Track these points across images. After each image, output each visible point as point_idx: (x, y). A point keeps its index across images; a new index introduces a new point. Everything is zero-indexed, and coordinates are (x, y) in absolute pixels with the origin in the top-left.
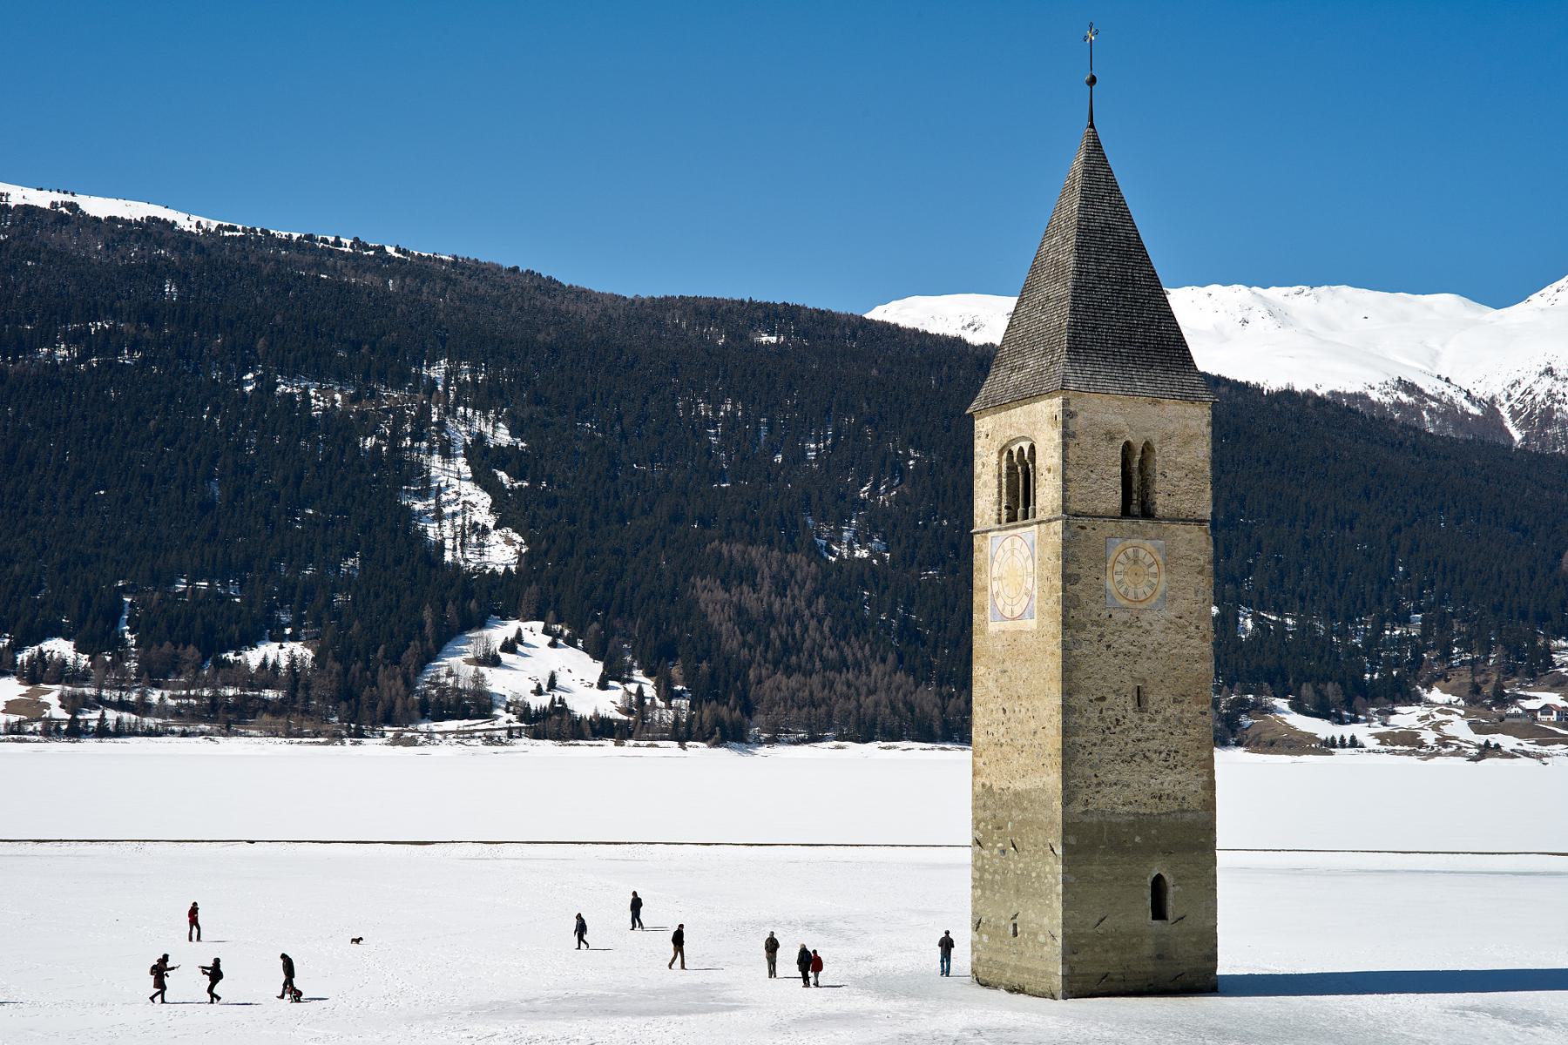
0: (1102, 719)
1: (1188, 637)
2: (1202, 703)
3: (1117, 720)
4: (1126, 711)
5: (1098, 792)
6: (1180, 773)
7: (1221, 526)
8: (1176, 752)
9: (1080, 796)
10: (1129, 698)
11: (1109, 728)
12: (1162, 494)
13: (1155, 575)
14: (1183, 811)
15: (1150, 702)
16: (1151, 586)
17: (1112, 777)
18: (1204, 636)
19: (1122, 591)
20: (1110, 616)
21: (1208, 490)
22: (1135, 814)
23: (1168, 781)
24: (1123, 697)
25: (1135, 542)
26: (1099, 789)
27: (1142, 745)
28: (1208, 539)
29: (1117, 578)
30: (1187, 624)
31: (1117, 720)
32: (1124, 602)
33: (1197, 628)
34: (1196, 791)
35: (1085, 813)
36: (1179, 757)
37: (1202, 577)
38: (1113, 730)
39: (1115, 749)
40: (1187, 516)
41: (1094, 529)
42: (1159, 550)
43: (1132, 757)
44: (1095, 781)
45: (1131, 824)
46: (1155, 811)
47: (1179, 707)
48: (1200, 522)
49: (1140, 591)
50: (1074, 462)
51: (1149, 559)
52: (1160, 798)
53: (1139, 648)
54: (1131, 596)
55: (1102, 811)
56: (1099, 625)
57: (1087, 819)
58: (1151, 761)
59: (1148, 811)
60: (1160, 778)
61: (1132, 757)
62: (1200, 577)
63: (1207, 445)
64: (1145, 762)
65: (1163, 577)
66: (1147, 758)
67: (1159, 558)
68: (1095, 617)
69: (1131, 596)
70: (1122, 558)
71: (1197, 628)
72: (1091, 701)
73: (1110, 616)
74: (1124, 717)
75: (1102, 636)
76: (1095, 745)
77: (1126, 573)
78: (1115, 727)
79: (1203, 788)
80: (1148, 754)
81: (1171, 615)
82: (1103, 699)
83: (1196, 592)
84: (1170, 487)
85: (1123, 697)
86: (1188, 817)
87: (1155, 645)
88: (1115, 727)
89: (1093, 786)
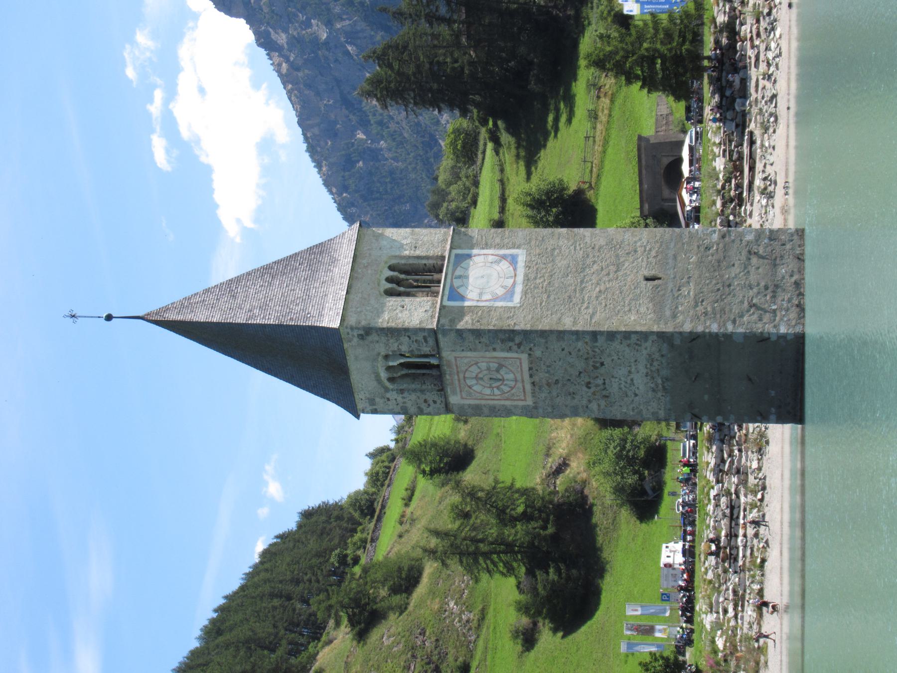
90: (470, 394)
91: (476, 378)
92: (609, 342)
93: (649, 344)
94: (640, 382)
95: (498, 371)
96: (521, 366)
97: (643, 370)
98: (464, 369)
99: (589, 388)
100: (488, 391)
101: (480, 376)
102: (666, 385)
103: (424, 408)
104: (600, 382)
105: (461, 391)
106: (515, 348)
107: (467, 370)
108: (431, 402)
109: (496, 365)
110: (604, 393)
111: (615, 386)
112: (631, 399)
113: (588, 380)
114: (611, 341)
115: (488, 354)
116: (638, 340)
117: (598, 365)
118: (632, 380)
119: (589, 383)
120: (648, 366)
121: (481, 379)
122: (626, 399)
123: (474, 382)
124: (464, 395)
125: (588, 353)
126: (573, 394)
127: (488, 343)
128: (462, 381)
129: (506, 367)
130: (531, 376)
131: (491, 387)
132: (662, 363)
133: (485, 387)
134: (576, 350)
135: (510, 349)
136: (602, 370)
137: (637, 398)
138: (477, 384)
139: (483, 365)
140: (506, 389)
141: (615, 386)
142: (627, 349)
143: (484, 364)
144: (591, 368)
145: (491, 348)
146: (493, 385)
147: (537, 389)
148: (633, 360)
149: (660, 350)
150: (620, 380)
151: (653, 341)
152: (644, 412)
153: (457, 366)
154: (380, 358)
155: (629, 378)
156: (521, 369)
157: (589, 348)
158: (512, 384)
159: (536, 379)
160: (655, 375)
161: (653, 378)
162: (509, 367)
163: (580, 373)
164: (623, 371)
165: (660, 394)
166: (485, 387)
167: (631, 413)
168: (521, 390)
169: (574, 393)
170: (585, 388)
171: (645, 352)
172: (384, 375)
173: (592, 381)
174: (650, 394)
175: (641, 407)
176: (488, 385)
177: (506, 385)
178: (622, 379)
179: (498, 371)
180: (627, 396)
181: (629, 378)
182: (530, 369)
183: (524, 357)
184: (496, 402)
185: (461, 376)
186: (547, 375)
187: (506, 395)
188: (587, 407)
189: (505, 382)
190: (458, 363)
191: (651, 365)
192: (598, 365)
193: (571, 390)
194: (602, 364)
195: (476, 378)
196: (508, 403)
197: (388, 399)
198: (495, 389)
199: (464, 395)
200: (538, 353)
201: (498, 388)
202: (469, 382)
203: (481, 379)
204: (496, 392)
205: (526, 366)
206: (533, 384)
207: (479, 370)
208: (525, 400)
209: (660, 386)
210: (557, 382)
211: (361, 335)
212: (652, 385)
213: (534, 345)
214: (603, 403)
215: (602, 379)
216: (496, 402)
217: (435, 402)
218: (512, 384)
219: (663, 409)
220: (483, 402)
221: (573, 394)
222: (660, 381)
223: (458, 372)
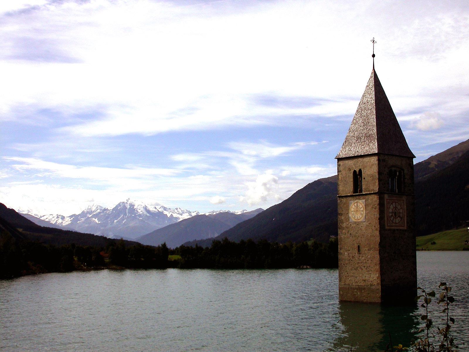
3: (353, 256)
4: (355, 254)
7: (380, 194)
8: (369, 266)
13: (362, 211)
16: (362, 215)
17: (352, 275)
18: (377, 229)
20: (351, 225)
21: (377, 182)
22: (358, 286)
23: (366, 276)
29: (352, 213)
31: (353, 256)
33: (375, 226)
35: (345, 284)
41: (346, 199)
42: (363, 203)
49: (358, 217)
50: (340, 179)
52: (365, 281)
54: (356, 218)
58: (362, 269)
64: (360, 270)
65: (365, 211)
67: (364, 205)
69: (356, 218)
70: (353, 207)
71: (375, 226)
73: (351, 225)
77: (354, 211)
82: (349, 250)
83: (374, 215)
84: (366, 183)
86: (373, 287)
91: (396, 207)
100: (390, 210)
101: (397, 209)
105: (390, 199)
107: (399, 204)
115: (405, 214)
118: (398, 271)
121: (396, 209)
123: (394, 206)
124: (388, 201)
129: (401, 220)
130: (397, 230)
131: (392, 213)
135: (407, 223)
138: (393, 207)
139: (401, 211)
140: (392, 219)
146: (393, 214)
153: (400, 200)
166: (392, 210)
168: (391, 225)
172: (393, 169)
176: (393, 211)
177: (393, 219)
182: (401, 230)
183: (405, 228)
184: (386, 214)
185: (396, 201)
187: (389, 218)
189: (394, 219)
195: (396, 207)
196: (386, 218)
197: (385, 168)
198: (392, 214)
199: (388, 201)
201: (392, 215)
203: (396, 209)
204: (390, 214)
205: (401, 228)
206: (394, 230)
207: (399, 209)
216: (386, 214)
220: (386, 208)
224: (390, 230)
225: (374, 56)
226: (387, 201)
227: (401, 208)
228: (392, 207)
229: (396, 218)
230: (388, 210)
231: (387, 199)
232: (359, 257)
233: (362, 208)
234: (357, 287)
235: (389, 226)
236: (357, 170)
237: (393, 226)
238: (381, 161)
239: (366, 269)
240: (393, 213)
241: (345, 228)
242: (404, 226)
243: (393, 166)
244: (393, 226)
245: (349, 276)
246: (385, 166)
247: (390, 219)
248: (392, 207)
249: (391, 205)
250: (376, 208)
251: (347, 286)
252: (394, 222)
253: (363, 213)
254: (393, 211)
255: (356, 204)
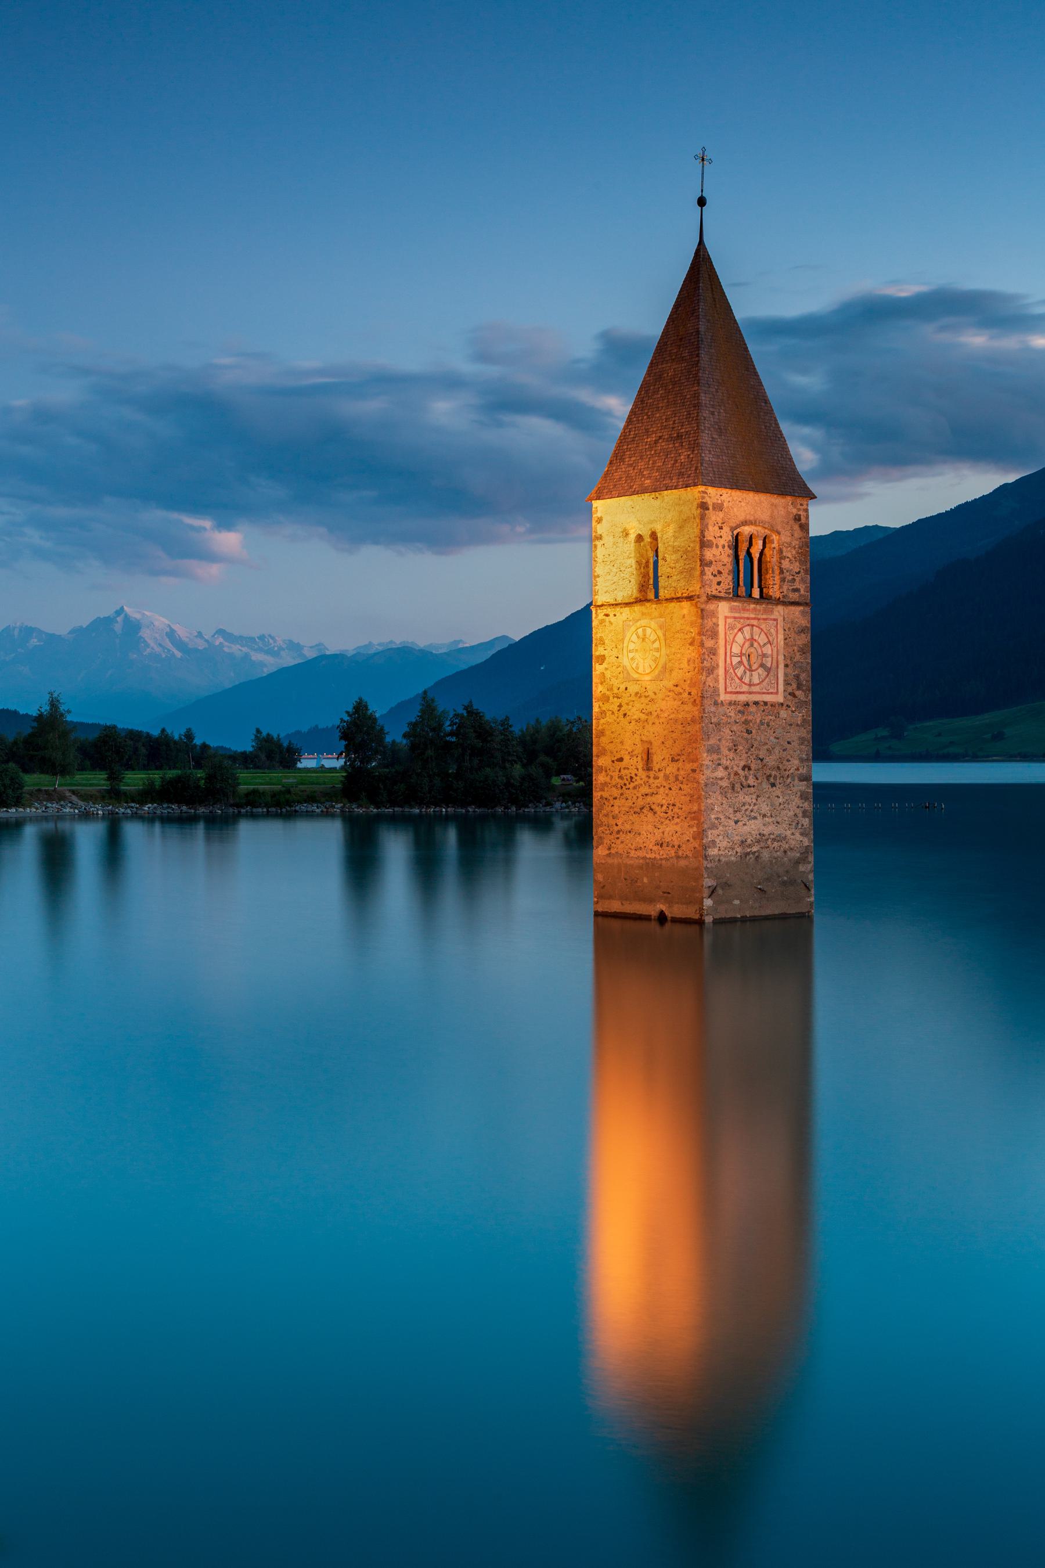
0: (621, 777)
1: (682, 703)
2: (693, 762)
3: (631, 778)
4: (638, 770)
5: (618, 838)
6: (677, 824)
8: (674, 805)
9: (605, 841)
10: (639, 758)
11: (625, 785)
12: (663, 577)
13: (658, 650)
14: (678, 857)
15: (654, 762)
16: (655, 661)
17: (628, 827)
18: (695, 700)
19: (634, 666)
20: (626, 689)
22: (644, 858)
24: (635, 758)
25: (643, 622)
26: (618, 836)
27: (649, 799)
28: (697, 611)
29: (631, 655)
30: (682, 691)
31: (631, 778)
32: (636, 676)
33: (690, 694)
34: (688, 841)
35: (609, 855)
36: (676, 810)
37: (693, 647)
38: (628, 786)
39: (629, 803)
40: (682, 594)
41: (615, 615)
43: (642, 809)
44: (616, 829)
45: (640, 867)
46: (658, 857)
47: (675, 765)
48: (690, 598)
51: (653, 637)
52: (661, 845)
53: (647, 715)
55: (620, 854)
56: (618, 698)
57: (610, 861)
59: (653, 856)
60: (662, 827)
61: (642, 809)
62: (691, 648)
63: (697, 526)
64: (650, 815)
65: (663, 649)
66: (652, 810)
67: (660, 633)
68: (615, 691)
69: (640, 670)
70: (634, 638)
71: (690, 694)
72: (613, 762)
73: (626, 689)
74: (636, 775)
75: (620, 706)
76: (615, 798)
78: (629, 784)
79: (694, 838)
80: (653, 807)
81: (669, 684)
82: (621, 760)
83: (689, 661)
85: (635, 758)
86: (683, 863)
87: (659, 712)
88: (629, 784)
89: (614, 834)
90: (732, 628)
91: (752, 640)
92: (799, 793)
93: (798, 837)
94: (752, 828)
95: (762, 665)
96: (768, 693)
97: (766, 831)
98: (763, 626)
99: (743, 769)
100: (736, 649)
101: (755, 645)
102: (751, 856)
103: (711, 569)
104: (751, 781)
105: (735, 618)
106: (790, 690)
108: (718, 579)
109: (769, 665)
110: (738, 786)
111: (748, 799)
112: (731, 816)
113: (753, 768)
114: (801, 796)
115: (781, 658)
116: (802, 825)
117: (772, 780)
118: (755, 818)
119: (749, 769)
120: (772, 836)
121: (752, 645)
122: (731, 810)
123: (748, 637)
124: (729, 621)
125: (785, 770)
126: (734, 748)
127: (795, 660)
128: (748, 622)
129: (768, 675)
130: (756, 703)
131: (741, 655)
132: (776, 852)
133: (742, 647)
134: (789, 757)
135: (787, 683)
136: (766, 786)
137: (733, 823)
138: (745, 638)
139: (768, 650)
140: (740, 672)
141: (748, 799)
142: (792, 813)
143: (770, 652)
144: (768, 772)
145: (789, 662)
146: (743, 658)
147: (739, 708)
148: (779, 820)
149: (791, 849)
150: (755, 804)
151: (801, 841)
152: (715, 832)
154: (767, 532)
155: (757, 815)
156: (764, 693)
157: (791, 771)
158: (746, 680)
159: (753, 709)
160: (762, 844)
161: (758, 842)
162: (767, 679)
163: (762, 760)
164: (765, 808)
165: (739, 850)
166: (742, 647)
167: (713, 817)
168: (738, 690)
169: (736, 750)
170: (742, 763)
171: (788, 833)
172: (747, 530)
173: (751, 772)
174: (737, 839)
175: (721, 828)
177: (745, 672)
178: (756, 807)
179: (762, 665)
180: (735, 812)
181: (757, 815)
182: (766, 703)
183: (780, 698)
185: (755, 622)
186: (758, 721)
187: (731, 671)
188: (719, 764)
189: (747, 671)
190: (771, 622)
191: (774, 840)
192: (772, 780)
193: (740, 748)
194: (773, 785)
195: (752, 640)
196: (721, 671)
197: (721, 528)
198: (739, 659)
199: (729, 621)
200: (783, 714)
201: (741, 663)
202: (747, 630)
203: (752, 645)
204: (736, 660)
206: (747, 704)
207: (762, 644)
208: (726, 692)
209: (749, 850)
210: (749, 732)
211: (799, 520)
212: (749, 841)
213: (793, 712)
214: (725, 783)
215: (755, 784)
217: (719, 583)
218: (746, 680)
219: (720, 853)
220: (721, 642)
221: (734, 748)
222: (754, 849)
223: (759, 619)
224: (730, 704)
225: (702, 202)
226: (726, 622)
227: (769, 642)
228: (740, 638)
229: (752, 671)
230: (728, 647)
231: (726, 617)
232: (647, 779)
233: (658, 642)
234: (641, 861)
235: (731, 693)
236: (646, 535)
237: (743, 693)
238: (709, 509)
239: (666, 813)
240: (745, 654)
241: (611, 698)
242: (777, 693)
243: (745, 523)
244: (743, 693)
245: (621, 833)
246: (722, 523)
247: (736, 674)
248: (740, 638)
249: (736, 634)
250: (694, 641)
251: (616, 861)
252: (747, 680)
253: (658, 656)
254: (744, 652)
255: (640, 631)
